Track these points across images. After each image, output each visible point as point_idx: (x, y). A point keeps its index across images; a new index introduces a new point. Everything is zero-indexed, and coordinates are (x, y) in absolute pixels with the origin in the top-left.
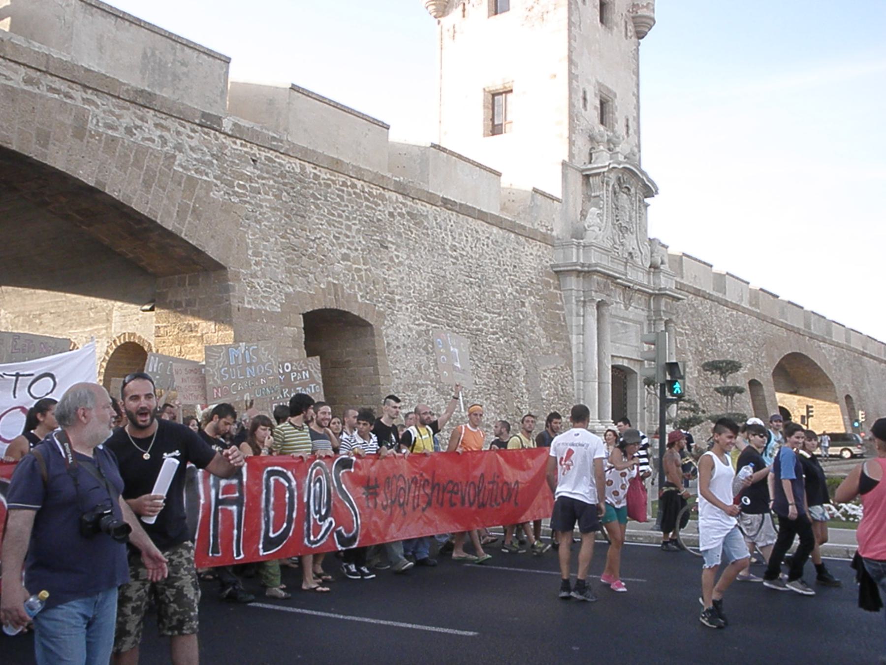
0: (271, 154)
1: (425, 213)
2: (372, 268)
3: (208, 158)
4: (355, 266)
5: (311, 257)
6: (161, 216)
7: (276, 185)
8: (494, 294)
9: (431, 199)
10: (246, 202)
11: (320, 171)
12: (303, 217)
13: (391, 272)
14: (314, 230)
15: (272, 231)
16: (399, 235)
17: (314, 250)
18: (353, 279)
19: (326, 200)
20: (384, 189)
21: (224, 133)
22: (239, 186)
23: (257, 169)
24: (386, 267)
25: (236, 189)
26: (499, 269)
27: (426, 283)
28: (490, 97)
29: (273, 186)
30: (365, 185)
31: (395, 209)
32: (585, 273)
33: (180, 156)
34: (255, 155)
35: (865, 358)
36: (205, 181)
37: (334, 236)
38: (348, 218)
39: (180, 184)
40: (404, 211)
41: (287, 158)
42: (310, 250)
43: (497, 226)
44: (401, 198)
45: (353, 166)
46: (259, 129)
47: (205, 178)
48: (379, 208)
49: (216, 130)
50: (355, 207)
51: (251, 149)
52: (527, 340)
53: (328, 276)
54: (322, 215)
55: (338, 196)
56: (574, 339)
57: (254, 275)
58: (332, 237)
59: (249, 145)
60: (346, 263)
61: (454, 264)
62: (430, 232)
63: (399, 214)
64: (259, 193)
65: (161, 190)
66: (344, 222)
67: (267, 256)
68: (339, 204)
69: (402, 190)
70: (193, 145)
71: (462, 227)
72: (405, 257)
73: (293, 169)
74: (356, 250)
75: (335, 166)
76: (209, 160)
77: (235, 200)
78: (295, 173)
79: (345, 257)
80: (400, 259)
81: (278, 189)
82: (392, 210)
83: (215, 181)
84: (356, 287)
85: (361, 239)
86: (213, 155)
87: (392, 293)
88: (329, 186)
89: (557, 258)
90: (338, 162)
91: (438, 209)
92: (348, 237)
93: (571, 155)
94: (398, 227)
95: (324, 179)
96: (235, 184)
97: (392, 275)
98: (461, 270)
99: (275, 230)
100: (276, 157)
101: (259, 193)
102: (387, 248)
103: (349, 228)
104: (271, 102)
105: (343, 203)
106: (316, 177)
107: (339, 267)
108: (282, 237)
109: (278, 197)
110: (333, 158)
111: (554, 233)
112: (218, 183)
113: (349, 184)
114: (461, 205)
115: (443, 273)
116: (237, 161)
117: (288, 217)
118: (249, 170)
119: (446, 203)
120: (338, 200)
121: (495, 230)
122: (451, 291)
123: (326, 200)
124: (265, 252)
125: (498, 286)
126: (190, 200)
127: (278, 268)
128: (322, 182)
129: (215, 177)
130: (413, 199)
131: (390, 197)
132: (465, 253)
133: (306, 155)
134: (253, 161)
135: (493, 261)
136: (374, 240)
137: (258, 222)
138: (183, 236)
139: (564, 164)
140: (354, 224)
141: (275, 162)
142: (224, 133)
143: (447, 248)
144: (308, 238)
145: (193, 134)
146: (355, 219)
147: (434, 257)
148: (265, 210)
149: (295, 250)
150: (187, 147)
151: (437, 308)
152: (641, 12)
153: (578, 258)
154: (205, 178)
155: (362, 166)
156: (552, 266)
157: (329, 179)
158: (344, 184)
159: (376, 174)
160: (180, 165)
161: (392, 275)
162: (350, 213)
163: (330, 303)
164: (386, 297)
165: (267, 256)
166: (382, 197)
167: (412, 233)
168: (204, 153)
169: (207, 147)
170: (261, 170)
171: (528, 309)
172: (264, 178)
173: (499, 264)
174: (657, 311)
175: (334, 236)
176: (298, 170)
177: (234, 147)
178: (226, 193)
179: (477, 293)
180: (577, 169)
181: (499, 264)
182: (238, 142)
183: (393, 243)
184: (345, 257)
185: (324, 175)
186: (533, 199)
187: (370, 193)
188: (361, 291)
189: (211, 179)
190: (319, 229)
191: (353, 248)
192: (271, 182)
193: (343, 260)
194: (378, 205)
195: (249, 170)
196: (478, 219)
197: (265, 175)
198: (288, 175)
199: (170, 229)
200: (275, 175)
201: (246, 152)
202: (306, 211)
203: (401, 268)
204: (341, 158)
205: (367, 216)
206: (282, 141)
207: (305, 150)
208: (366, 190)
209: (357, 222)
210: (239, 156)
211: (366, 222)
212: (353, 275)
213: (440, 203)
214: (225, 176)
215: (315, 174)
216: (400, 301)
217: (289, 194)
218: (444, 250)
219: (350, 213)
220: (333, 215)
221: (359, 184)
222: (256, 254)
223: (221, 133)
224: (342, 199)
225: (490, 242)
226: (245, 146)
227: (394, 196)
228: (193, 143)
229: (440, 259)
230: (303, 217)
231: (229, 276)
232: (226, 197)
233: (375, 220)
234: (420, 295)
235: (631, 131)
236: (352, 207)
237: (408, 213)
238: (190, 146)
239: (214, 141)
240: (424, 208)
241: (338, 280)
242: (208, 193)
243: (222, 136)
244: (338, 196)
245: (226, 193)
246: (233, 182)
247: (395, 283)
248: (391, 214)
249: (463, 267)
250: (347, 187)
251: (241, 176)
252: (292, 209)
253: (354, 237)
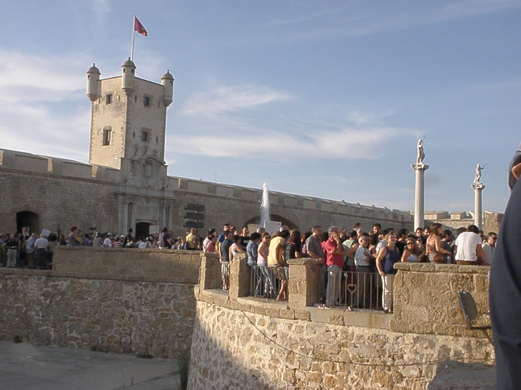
0: (10, 173)
9: (63, 177)
32: (124, 194)
35: (335, 215)
52: (98, 216)
56: (120, 215)
75: (30, 173)
90: (30, 172)
93: (126, 155)
103: (33, 189)
106: (24, 177)
111: (116, 181)
118: (3, 178)
119: (69, 178)
121: (89, 183)
133: (19, 172)
137: (5, 191)
139: (122, 158)
152: (166, 98)
156: (114, 192)
158: (33, 177)
163: (25, 209)
166: (46, 179)
171: (100, 206)
180: (128, 159)
184: (31, 197)
185: (26, 176)
187: (41, 179)
195: (3, 178)
221: (37, 177)
227: (49, 178)
235: (159, 141)
248: (48, 184)
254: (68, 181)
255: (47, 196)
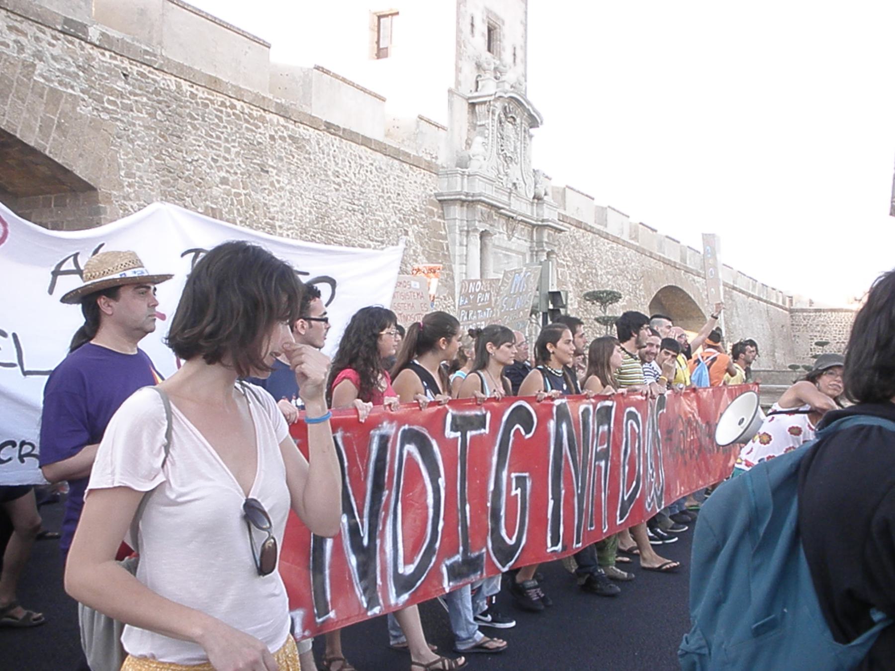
0: (145, 69)
1: (308, 137)
2: (252, 193)
3: (73, 69)
4: (234, 190)
5: (188, 179)
6: (21, 130)
7: (150, 103)
8: (377, 222)
9: (313, 123)
10: (117, 119)
11: (197, 89)
12: (179, 137)
13: (271, 197)
14: (191, 152)
15: (146, 152)
16: (281, 159)
17: (192, 173)
18: (232, 204)
19: (203, 120)
20: (265, 110)
21: (91, 43)
22: (109, 101)
23: (128, 84)
24: (267, 191)
25: (106, 105)
26: (383, 197)
27: (307, 209)
28: (376, 18)
29: (146, 104)
30: (245, 105)
31: (276, 132)
32: (469, 203)
33: (40, 65)
34: (125, 69)
36: (71, 95)
37: (213, 159)
38: (227, 140)
39: (41, 96)
40: (285, 134)
41: (161, 74)
42: (187, 173)
43: (380, 152)
44: (282, 121)
45: (232, 85)
46: (129, 41)
47: (70, 91)
48: (259, 130)
49: (82, 39)
50: (235, 129)
51: (122, 62)
53: (206, 200)
54: (199, 136)
55: (217, 116)
57: (127, 198)
58: (210, 159)
59: (119, 58)
60: (224, 187)
61: (337, 190)
62: (312, 157)
63: (280, 137)
64: (132, 110)
65: (20, 102)
66: (223, 145)
67: (140, 177)
68: (218, 125)
69: (283, 112)
70: (55, 53)
71: (345, 152)
72: (286, 182)
73: (168, 86)
74: (236, 173)
75: (214, 84)
76: (74, 73)
77: (105, 116)
78: (170, 90)
79: (224, 181)
80: (282, 184)
81: (152, 107)
82: (273, 133)
83: (82, 95)
84: (235, 212)
85: (241, 163)
86: (78, 67)
87: (273, 219)
88: (207, 106)
89: (443, 187)
90: (216, 81)
91: (321, 133)
92: (227, 160)
93: (458, 83)
94: (279, 151)
95: (201, 98)
96: (105, 99)
97: (272, 201)
98: (344, 196)
99: (149, 150)
100: (149, 72)
101: (132, 110)
102: (267, 172)
103: (228, 150)
104: (143, 12)
105: (222, 125)
106: (193, 96)
107: (216, 191)
108: (157, 158)
109: (152, 115)
110: (210, 76)
111: (439, 162)
112: (86, 97)
113: (228, 104)
114: (344, 130)
115: (324, 199)
116: (107, 75)
117: (163, 137)
120: (216, 120)
121: (379, 156)
122: (333, 218)
123: (203, 120)
124: (138, 174)
125: (382, 214)
126: (54, 114)
127: (152, 190)
128: (199, 101)
129: (82, 91)
130: (295, 122)
131: (271, 120)
132: (347, 179)
133: (181, 72)
134: (125, 75)
135: (377, 188)
136: (254, 164)
137: (131, 141)
138: (47, 153)
139: (450, 91)
140: (233, 147)
141: (148, 77)
142: (91, 43)
143: (330, 173)
144: (184, 160)
145: (54, 42)
146: (234, 141)
147: (316, 183)
148: (138, 128)
149: (170, 172)
150: (49, 56)
151: (319, 235)
153: (462, 188)
154: (70, 91)
155: (242, 86)
156: (436, 195)
157: (206, 99)
158: (223, 104)
159: (256, 95)
160: (41, 75)
161: (272, 201)
162: (229, 135)
164: (267, 223)
165: (140, 177)
166: (263, 120)
167: (293, 157)
168: (68, 64)
169: (72, 58)
170: (133, 85)
172: (136, 95)
173: (383, 191)
174: (540, 242)
175: (213, 159)
176: (173, 88)
177: (103, 59)
178: (94, 109)
179: (360, 221)
181: (383, 191)
182: (107, 53)
183: (274, 168)
184: (224, 181)
185: (201, 93)
186: (418, 126)
187: (250, 115)
188: (240, 216)
189: (77, 92)
190: (197, 150)
191: (232, 171)
192: (145, 99)
193: (222, 183)
194: (258, 127)
195: (120, 85)
196: (362, 144)
197: (138, 91)
198: (162, 92)
199: (32, 144)
200: (148, 92)
201: (116, 66)
202: (182, 132)
203: (282, 194)
204: (218, 76)
205: (247, 139)
206: (155, 56)
207: (180, 66)
208: (246, 111)
209: (237, 144)
210: (109, 70)
211: (245, 144)
212: (232, 199)
213: (323, 127)
214: (93, 91)
215: (191, 92)
216: (280, 227)
217: (163, 112)
218: (327, 175)
219: (229, 135)
220: (211, 136)
222: (128, 175)
223: (86, 42)
224: (220, 119)
225: (373, 168)
226: (115, 59)
227: (275, 118)
228: (56, 51)
229: (323, 185)
230: (179, 137)
231: (100, 198)
232: (95, 113)
233: (255, 143)
234: (302, 221)
236: (232, 129)
237: (290, 136)
238: (52, 55)
239: (78, 51)
240: (305, 132)
241: (216, 204)
242: (74, 108)
243: (88, 46)
244: (217, 116)
245: (94, 109)
246: (102, 97)
247: (275, 209)
248: (272, 138)
249: (345, 194)
250: (226, 107)
251: (111, 91)
252: (168, 129)
253: (233, 160)
254: (328, 138)
255: (272, 184)
